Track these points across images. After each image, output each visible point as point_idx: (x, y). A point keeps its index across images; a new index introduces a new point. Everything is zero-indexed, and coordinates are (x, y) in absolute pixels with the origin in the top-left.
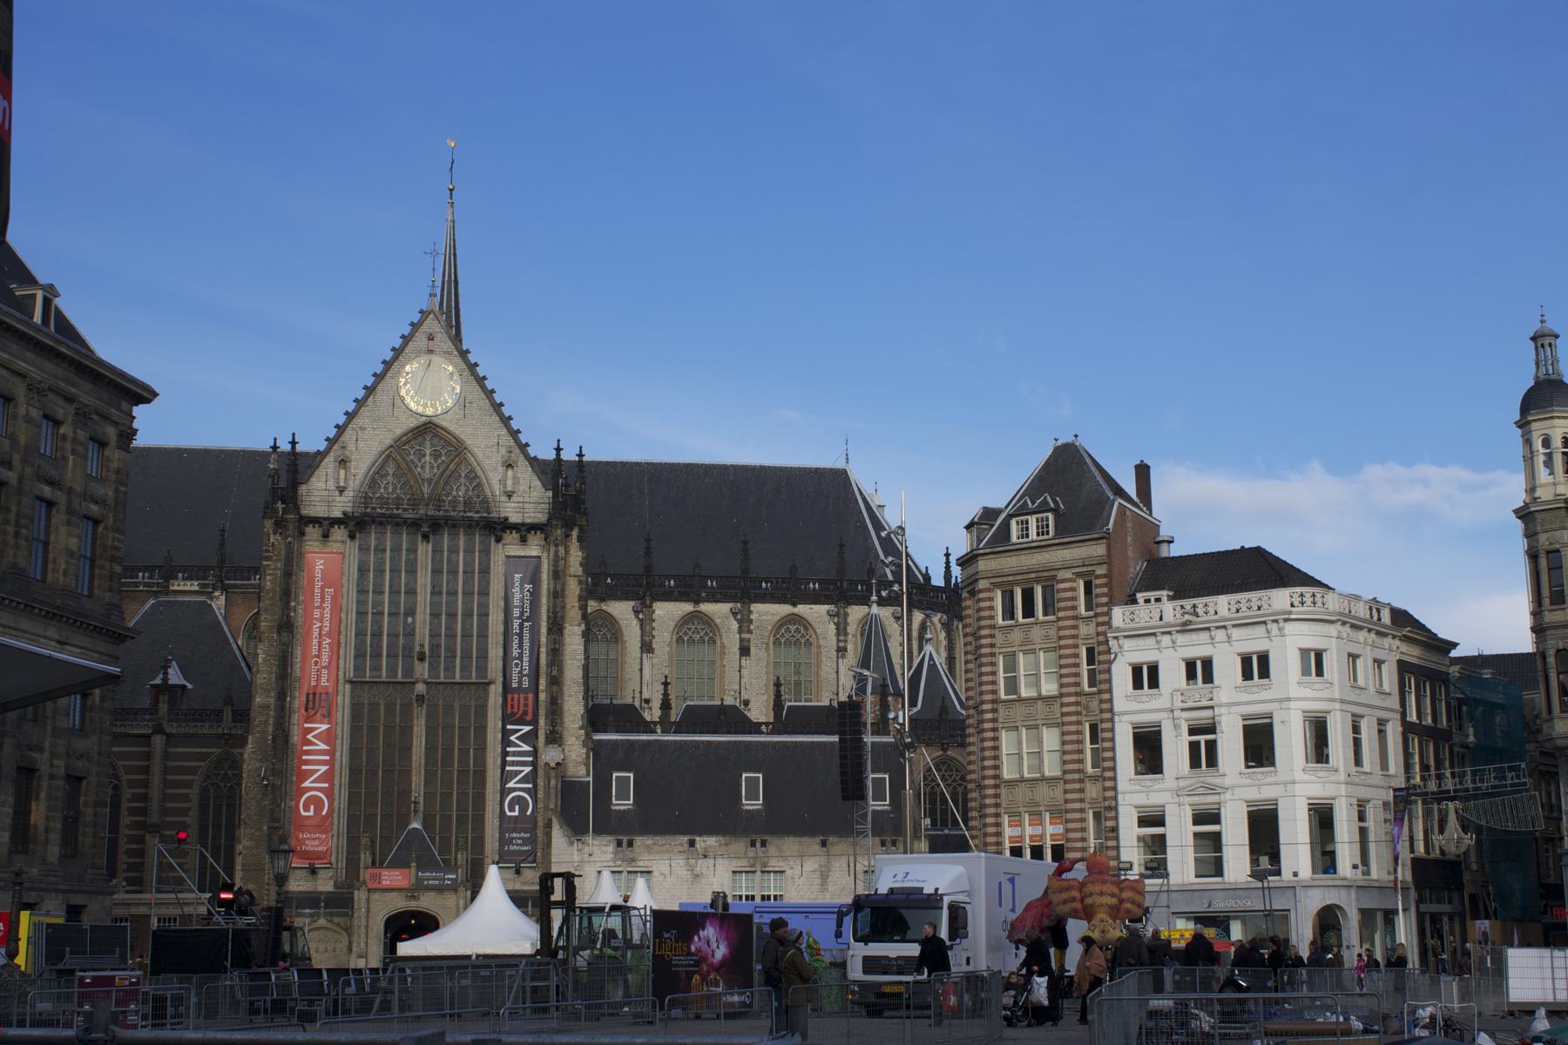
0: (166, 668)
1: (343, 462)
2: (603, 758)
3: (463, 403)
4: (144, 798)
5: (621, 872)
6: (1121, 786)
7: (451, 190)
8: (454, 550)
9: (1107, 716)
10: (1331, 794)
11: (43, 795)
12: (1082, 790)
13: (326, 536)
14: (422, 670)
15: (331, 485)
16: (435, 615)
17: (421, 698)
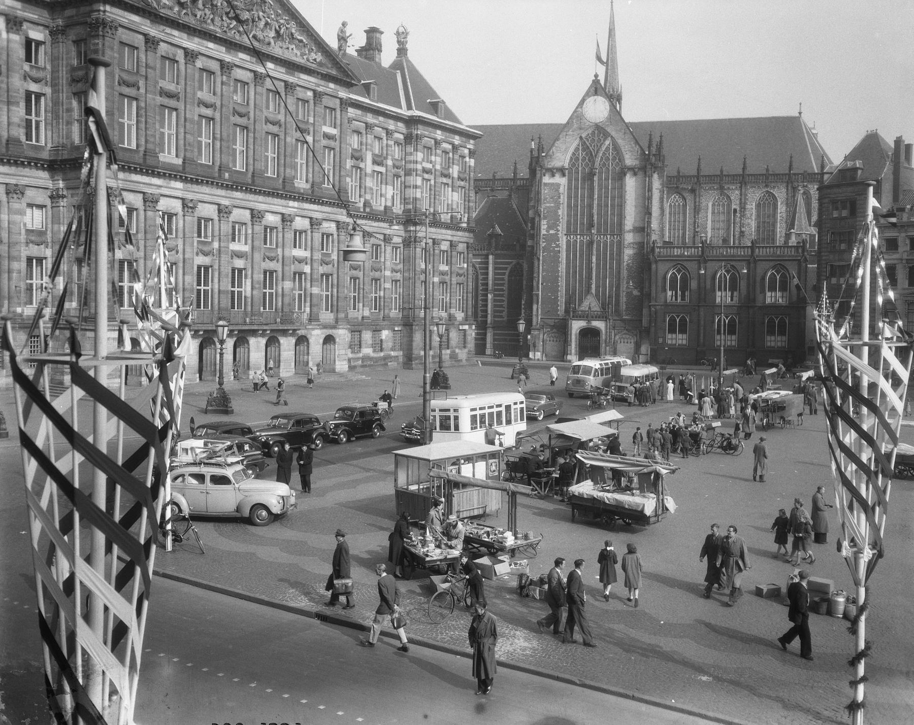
11: (448, 291)
13: (553, 176)
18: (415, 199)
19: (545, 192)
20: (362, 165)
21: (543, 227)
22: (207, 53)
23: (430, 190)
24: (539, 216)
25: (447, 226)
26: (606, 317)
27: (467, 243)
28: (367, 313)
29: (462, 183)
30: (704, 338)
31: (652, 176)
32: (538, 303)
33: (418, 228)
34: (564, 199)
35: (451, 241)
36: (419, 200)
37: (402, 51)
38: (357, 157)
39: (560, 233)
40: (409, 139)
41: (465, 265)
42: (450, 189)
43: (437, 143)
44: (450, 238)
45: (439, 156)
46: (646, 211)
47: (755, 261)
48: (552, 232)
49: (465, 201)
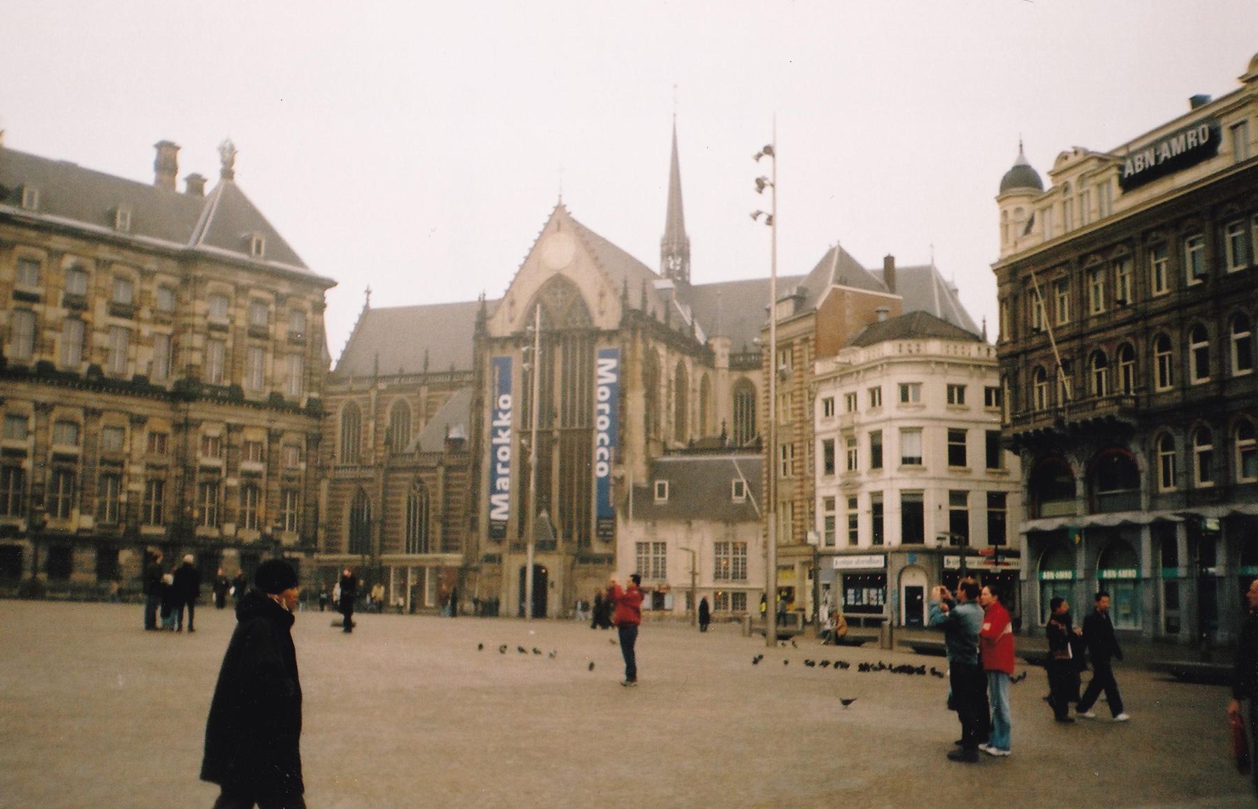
0: (447, 429)
1: (512, 303)
2: (655, 469)
4: (435, 502)
5: (647, 544)
6: (819, 483)
8: (574, 349)
9: (812, 436)
10: (968, 488)
11: (263, 500)
12: (802, 487)
13: (503, 347)
14: (557, 423)
15: (507, 318)
16: (564, 392)
17: (555, 441)
18: (191, 366)
20: (86, 316)
23: (226, 354)
25: (257, 406)
27: (307, 433)
28: (87, 522)
29: (299, 348)
33: (192, 406)
35: (269, 429)
36: (198, 367)
38: (77, 305)
40: (186, 281)
41: (303, 466)
42: (269, 356)
43: (241, 290)
44: (264, 423)
45: (241, 307)
49: (304, 374)
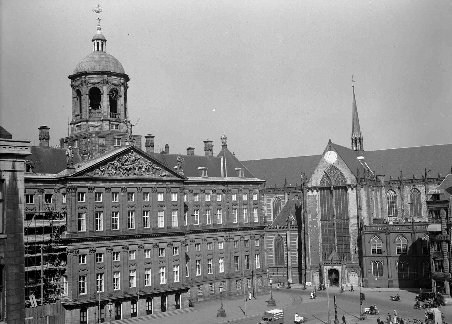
3: (338, 161)
7: (353, 87)
13: (312, 192)
19: (309, 201)
21: (309, 218)
22: (116, 186)
24: (306, 212)
26: (341, 264)
30: (391, 274)
31: (360, 190)
32: (309, 257)
34: (319, 203)
37: (224, 146)
39: (318, 220)
44: (249, 233)
46: (359, 208)
47: (414, 233)
48: (314, 220)
